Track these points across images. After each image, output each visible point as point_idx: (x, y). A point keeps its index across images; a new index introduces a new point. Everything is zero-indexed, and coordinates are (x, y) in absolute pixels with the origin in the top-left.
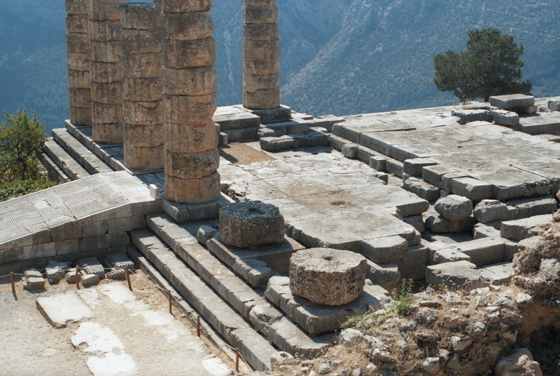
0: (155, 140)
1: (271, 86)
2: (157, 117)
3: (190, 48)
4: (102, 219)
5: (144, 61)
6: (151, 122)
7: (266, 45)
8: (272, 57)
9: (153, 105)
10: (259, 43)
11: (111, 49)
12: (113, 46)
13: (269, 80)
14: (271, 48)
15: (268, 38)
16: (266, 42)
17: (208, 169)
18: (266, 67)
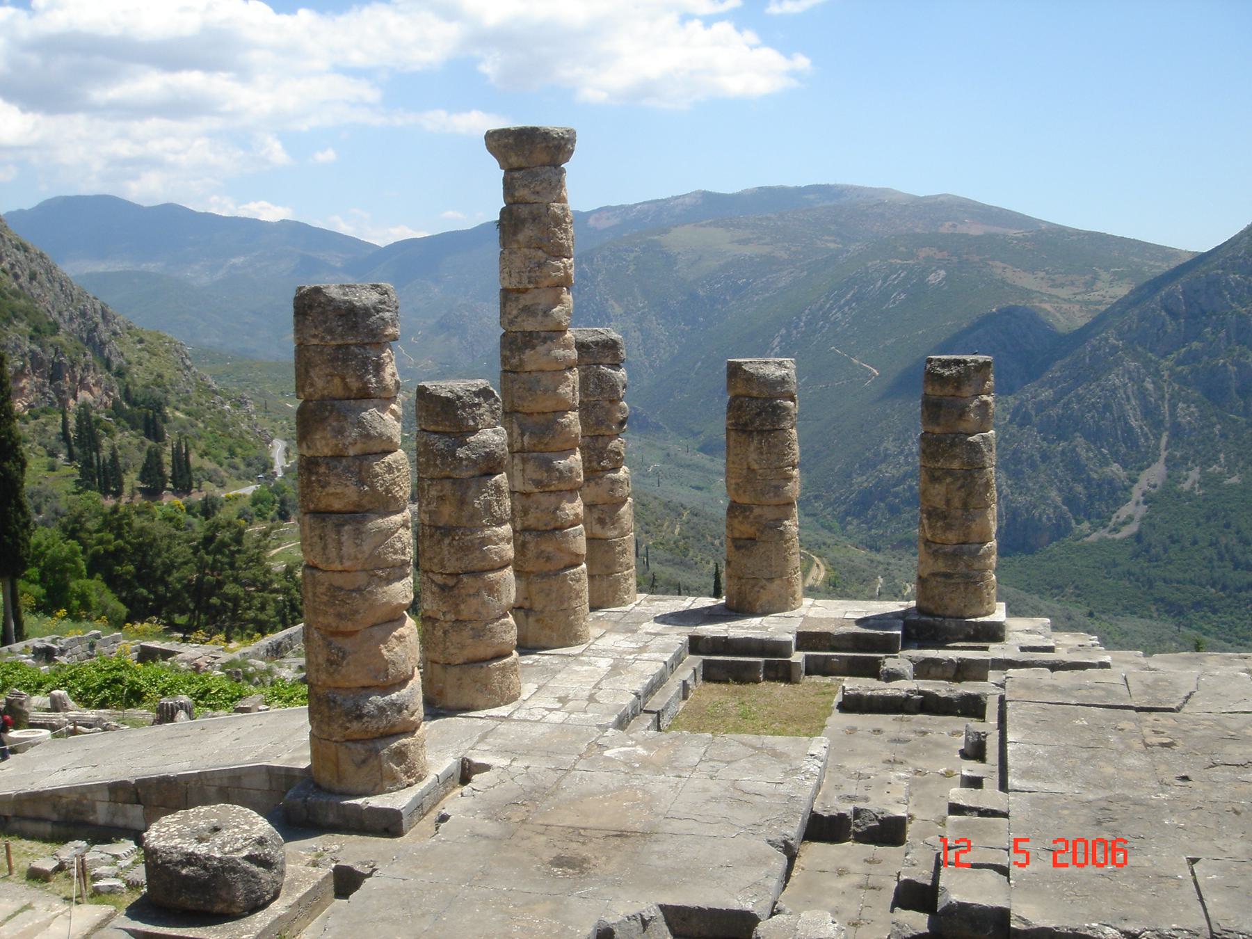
0: (452, 651)
1: (962, 568)
2: (457, 605)
3: (317, 473)
4: (217, 782)
5: (433, 493)
6: (444, 614)
7: (949, 480)
8: (965, 506)
9: (451, 582)
10: (937, 474)
11: (520, 467)
12: (524, 461)
13: (955, 556)
14: (962, 487)
15: (956, 465)
16: (949, 472)
17: (355, 726)
18: (948, 527)
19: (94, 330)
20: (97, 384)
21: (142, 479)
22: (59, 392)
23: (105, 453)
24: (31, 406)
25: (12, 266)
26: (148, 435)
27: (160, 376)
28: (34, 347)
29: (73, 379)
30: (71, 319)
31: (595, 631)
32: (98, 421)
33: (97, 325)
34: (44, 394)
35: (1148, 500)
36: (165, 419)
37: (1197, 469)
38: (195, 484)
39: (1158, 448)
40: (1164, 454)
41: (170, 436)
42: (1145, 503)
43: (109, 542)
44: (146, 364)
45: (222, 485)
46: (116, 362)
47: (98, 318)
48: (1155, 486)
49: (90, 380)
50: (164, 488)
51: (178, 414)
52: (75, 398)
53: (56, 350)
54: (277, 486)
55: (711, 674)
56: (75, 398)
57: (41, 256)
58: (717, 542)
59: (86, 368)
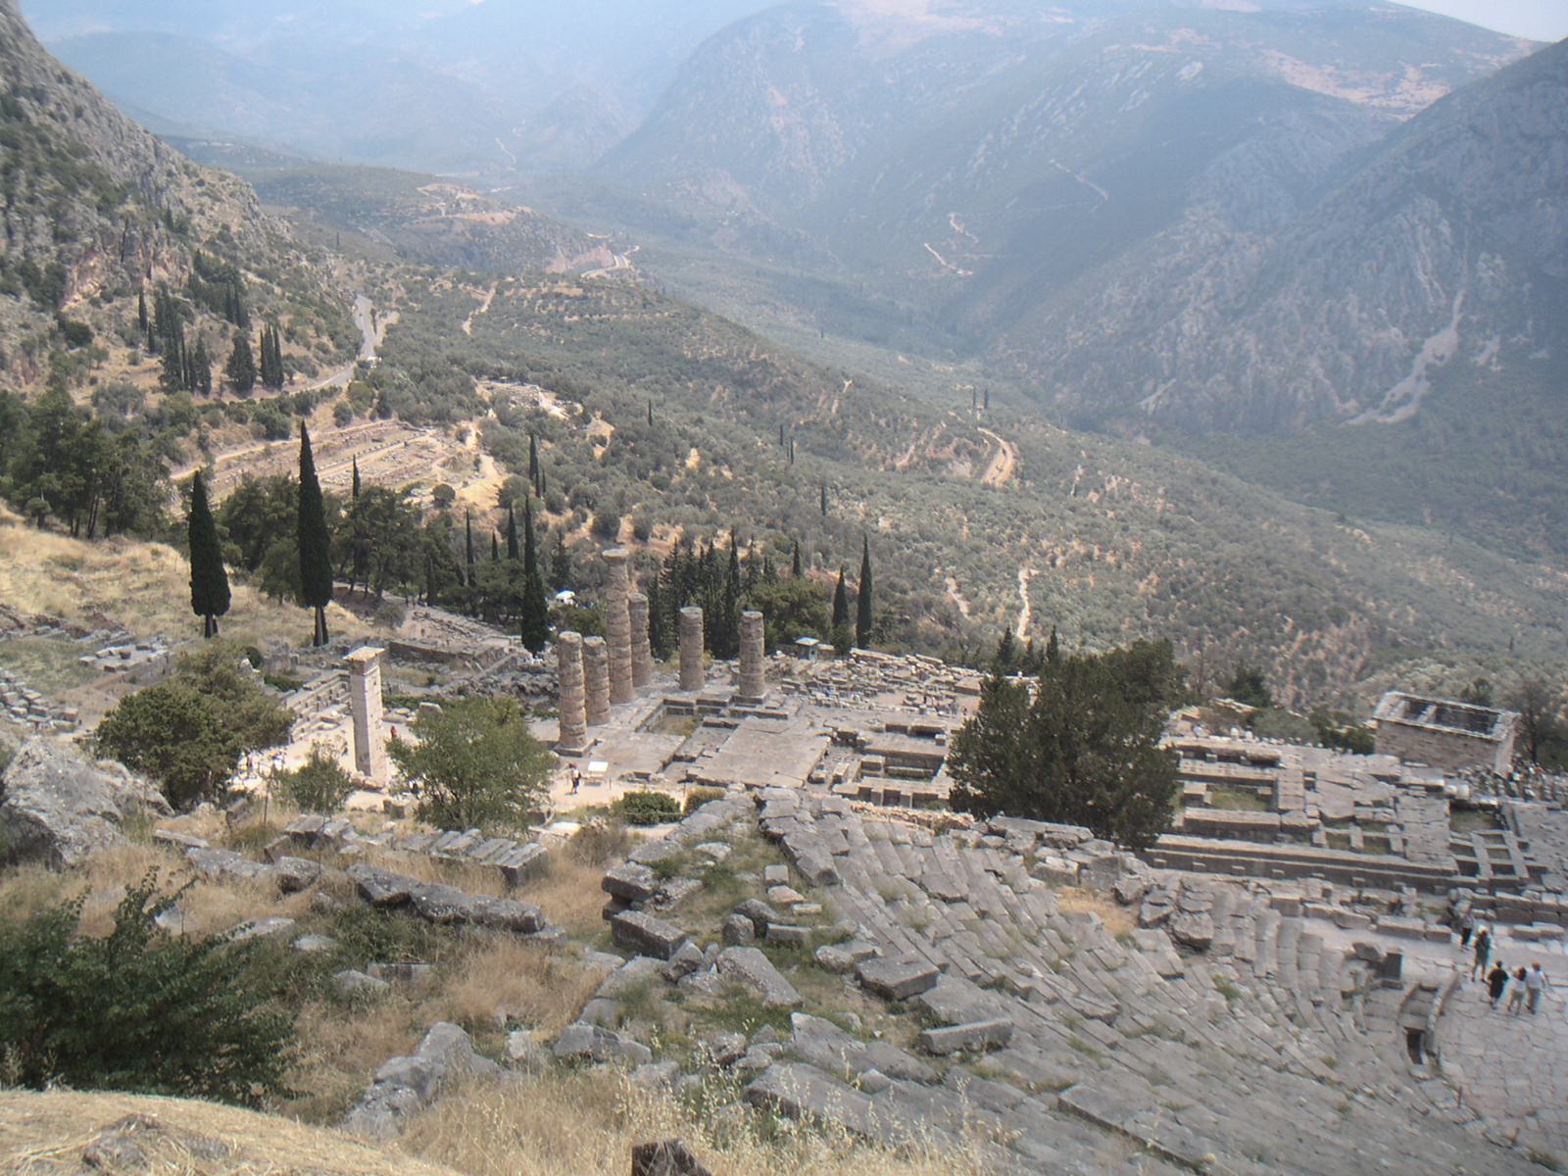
19: (147, 174)
22: (132, 270)
24: (103, 288)
26: (229, 319)
27: (226, 227)
29: (146, 254)
30: (122, 160)
31: (635, 696)
32: (177, 303)
33: (152, 167)
34: (116, 273)
35: (1433, 374)
37: (1497, 339)
38: (286, 376)
39: (1449, 308)
40: (1457, 318)
41: (257, 330)
42: (1428, 378)
43: (282, 509)
44: (207, 210)
45: (313, 374)
46: (176, 211)
47: (152, 160)
48: (1442, 358)
49: (164, 255)
50: (253, 380)
52: (149, 276)
53: (127, 222)
54: (374, 376)
55: (669, 712)
56: (149, 276)
57: (85, 85)
58: (882, 422)
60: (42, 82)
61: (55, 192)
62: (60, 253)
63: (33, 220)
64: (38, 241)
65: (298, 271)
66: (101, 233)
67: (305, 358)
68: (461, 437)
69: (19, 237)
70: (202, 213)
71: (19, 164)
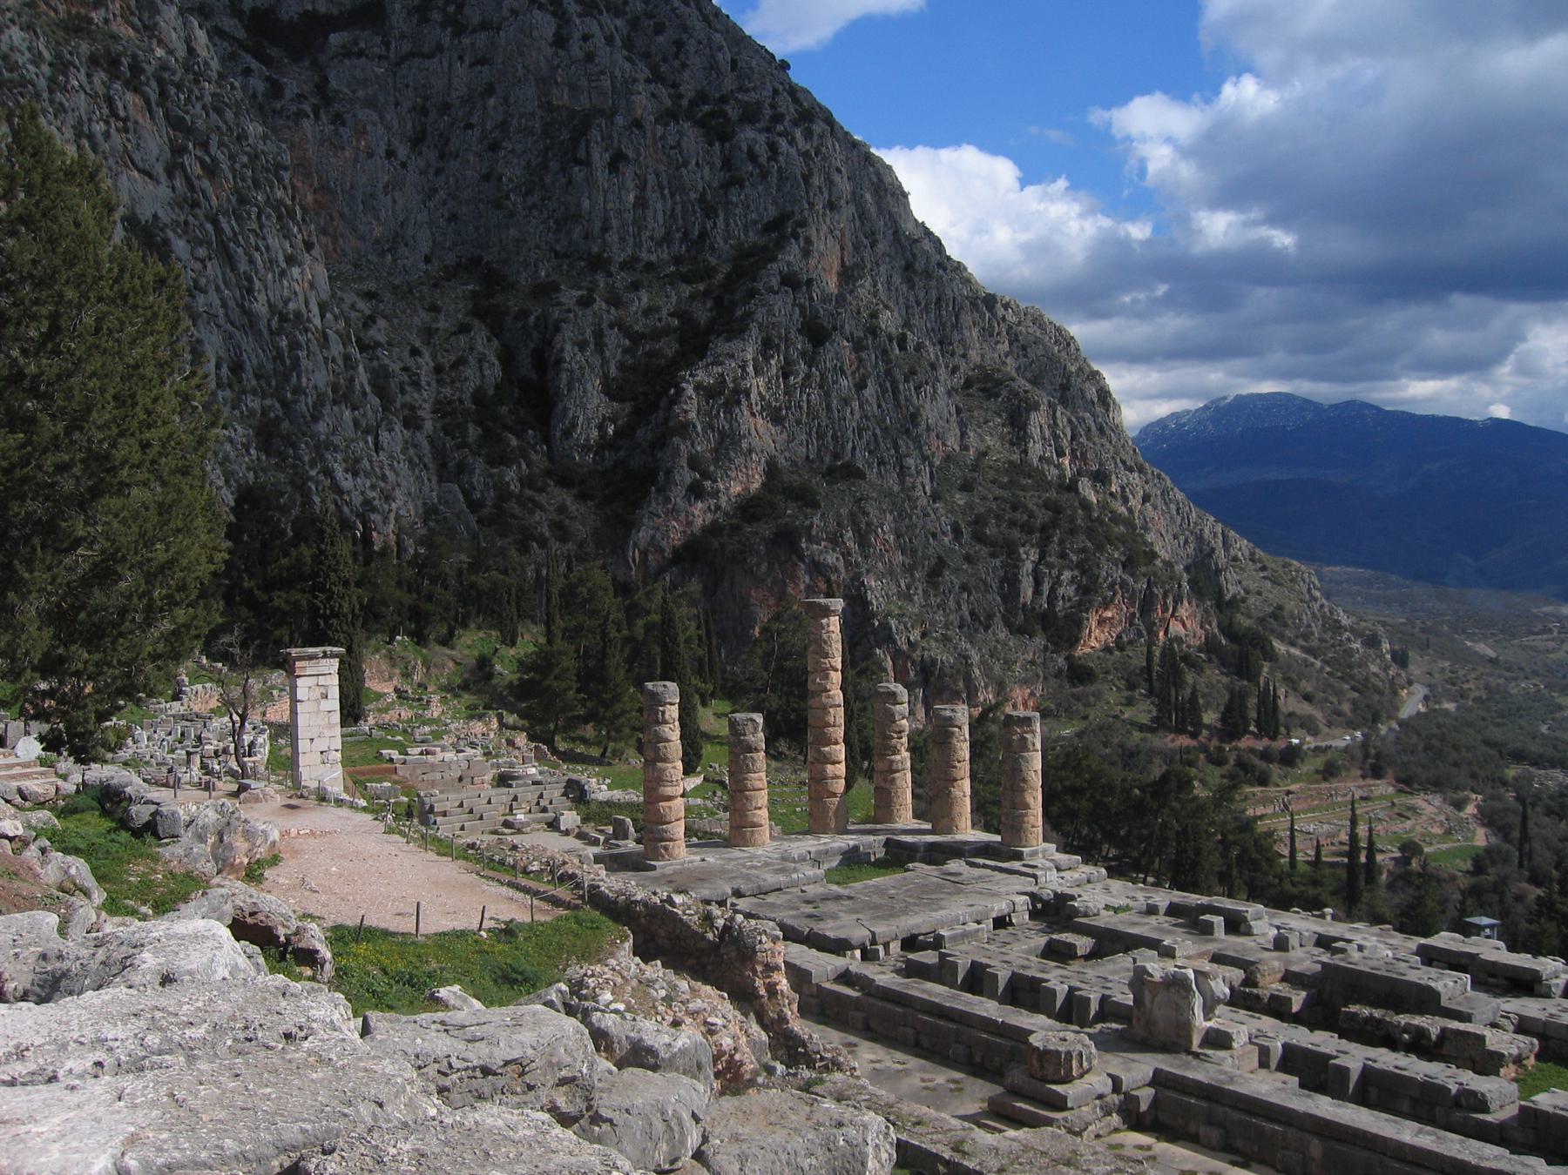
20: (1192, 616)
21: (1223, 719)
23: (1189, 690)
25: (1123, 488)
27: (1280, 608)
28: (1125, 577)
29: (1165, 610)
30: (1186, 542)
33: (1213, 550)
36: (1271, 656)
38: (1282, 729)
45: (1314, 732)
46: (1231, 590)
51: (1296, 652)
59: (1178, 600)
60: (1110, 466)
61: (1084, 550)
62: (1080, 603)
63: (1060, 574)
64: (1061, 591)
65: (1349, 652)
66: (1121, 587)
67: (1310, 717)
68: (1459, 805)
69: (1046, 588)
70: (1259, 593)
71: (1054, 523)
